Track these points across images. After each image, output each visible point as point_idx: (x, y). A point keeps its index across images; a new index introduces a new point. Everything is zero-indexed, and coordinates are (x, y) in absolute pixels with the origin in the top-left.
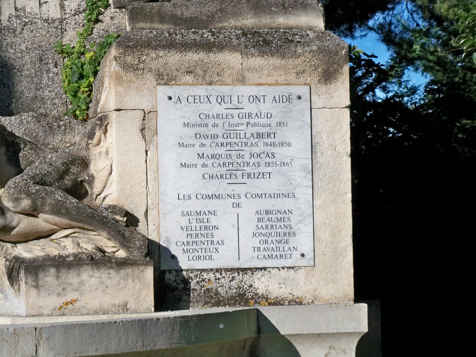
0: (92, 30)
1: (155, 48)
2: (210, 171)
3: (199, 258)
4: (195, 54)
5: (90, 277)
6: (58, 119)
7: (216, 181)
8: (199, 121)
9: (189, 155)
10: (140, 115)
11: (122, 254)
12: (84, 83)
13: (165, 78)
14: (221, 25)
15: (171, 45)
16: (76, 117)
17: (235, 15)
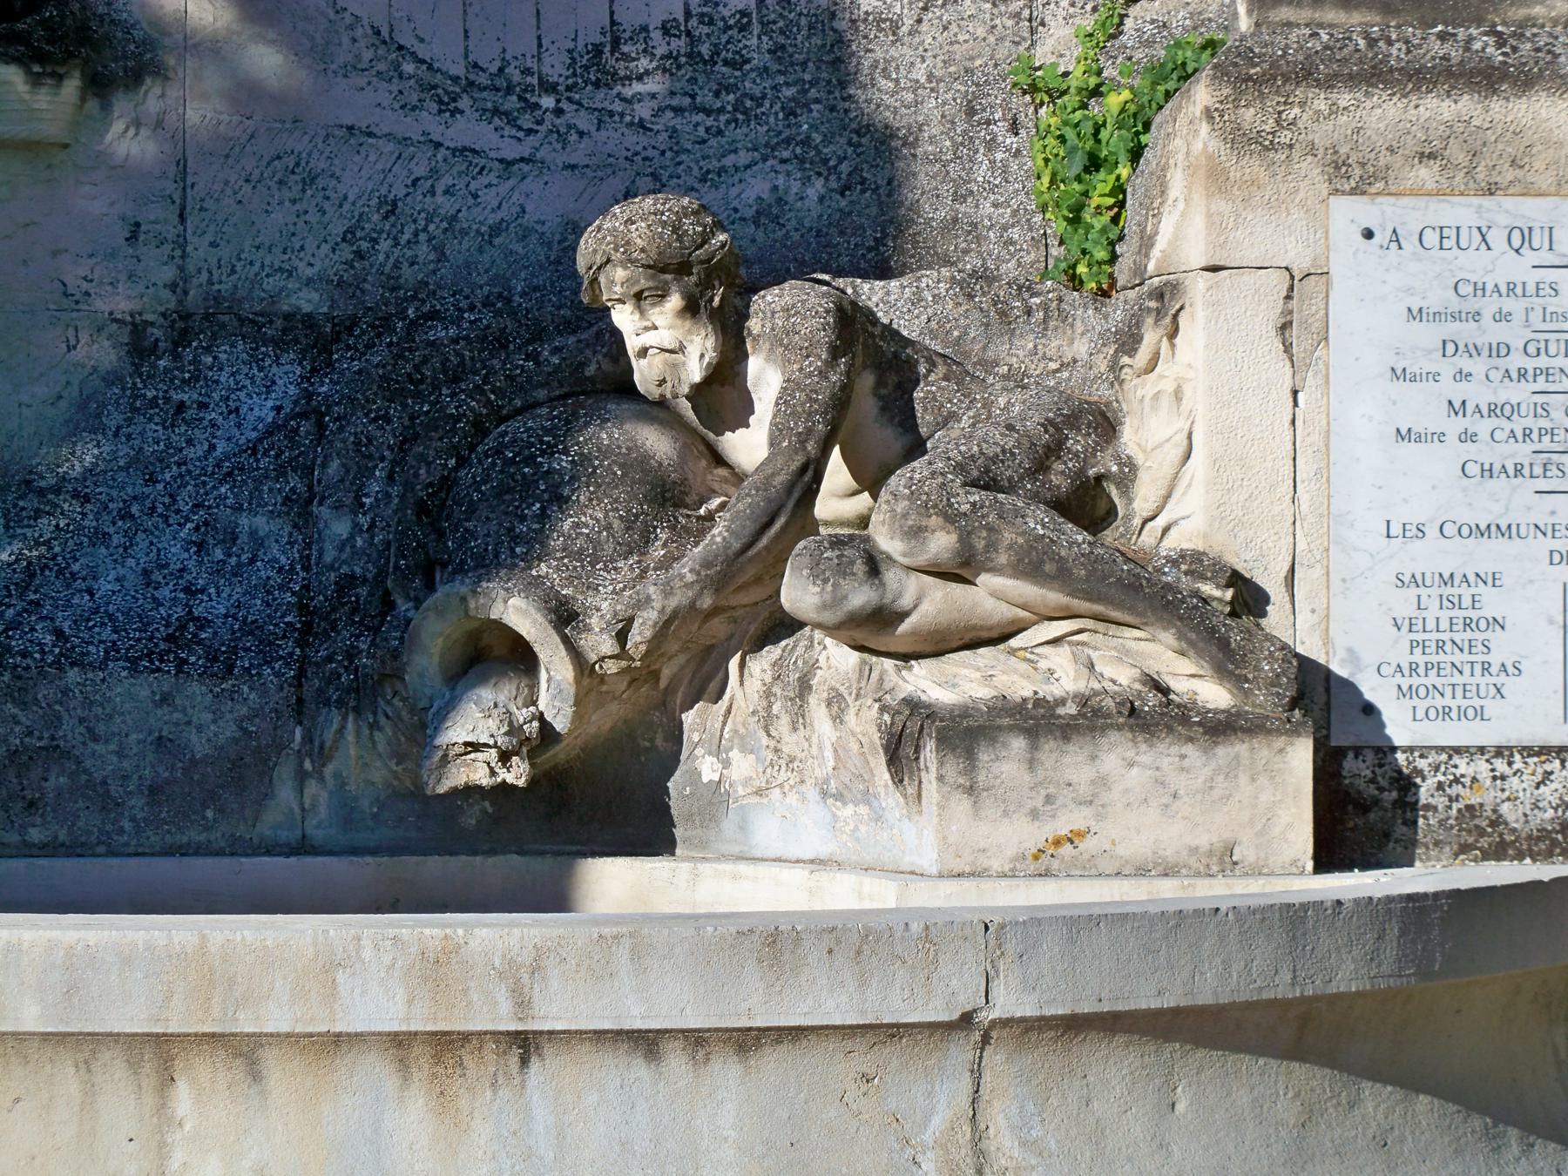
0: (1121, 23)
1: (1328, 84)
2: (1484, 453)
3: (1446, 712)
4: (1447, 102)
5: (1124, 763)
6: (1025, 288)
7: (1500, 484)
8: (1455, 304)
9: (1422, 406)
10: (1279, 282)
11: (1215, 695)
12: (1102, 183)
13: (1353, 174)
14: (1522, 13)
16: (1075, 282)
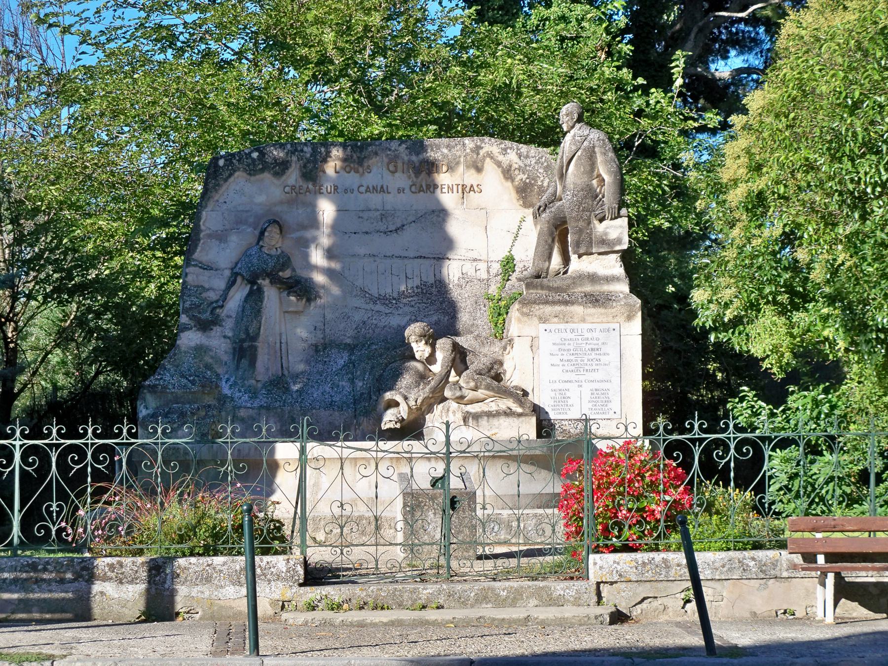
1: (539, 304)
2: (566, 368)
5: (504, 421)
6: (487, 338)
11: (520, 410)
12: (501, 318)
13: (543, 320)
15: (547, 302)
16: (496, 337)
17: (581, 285)
